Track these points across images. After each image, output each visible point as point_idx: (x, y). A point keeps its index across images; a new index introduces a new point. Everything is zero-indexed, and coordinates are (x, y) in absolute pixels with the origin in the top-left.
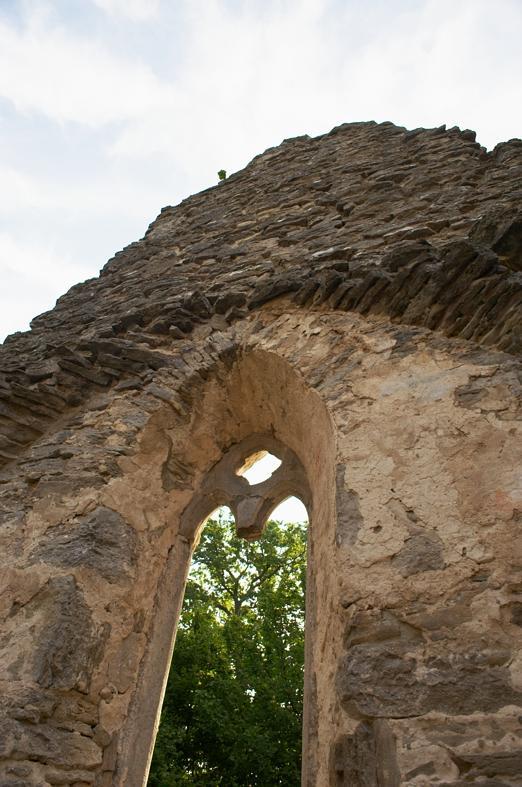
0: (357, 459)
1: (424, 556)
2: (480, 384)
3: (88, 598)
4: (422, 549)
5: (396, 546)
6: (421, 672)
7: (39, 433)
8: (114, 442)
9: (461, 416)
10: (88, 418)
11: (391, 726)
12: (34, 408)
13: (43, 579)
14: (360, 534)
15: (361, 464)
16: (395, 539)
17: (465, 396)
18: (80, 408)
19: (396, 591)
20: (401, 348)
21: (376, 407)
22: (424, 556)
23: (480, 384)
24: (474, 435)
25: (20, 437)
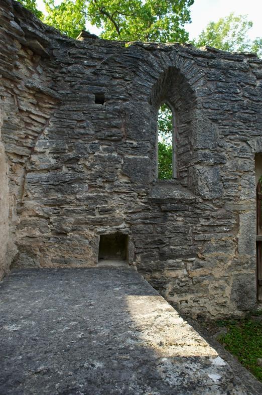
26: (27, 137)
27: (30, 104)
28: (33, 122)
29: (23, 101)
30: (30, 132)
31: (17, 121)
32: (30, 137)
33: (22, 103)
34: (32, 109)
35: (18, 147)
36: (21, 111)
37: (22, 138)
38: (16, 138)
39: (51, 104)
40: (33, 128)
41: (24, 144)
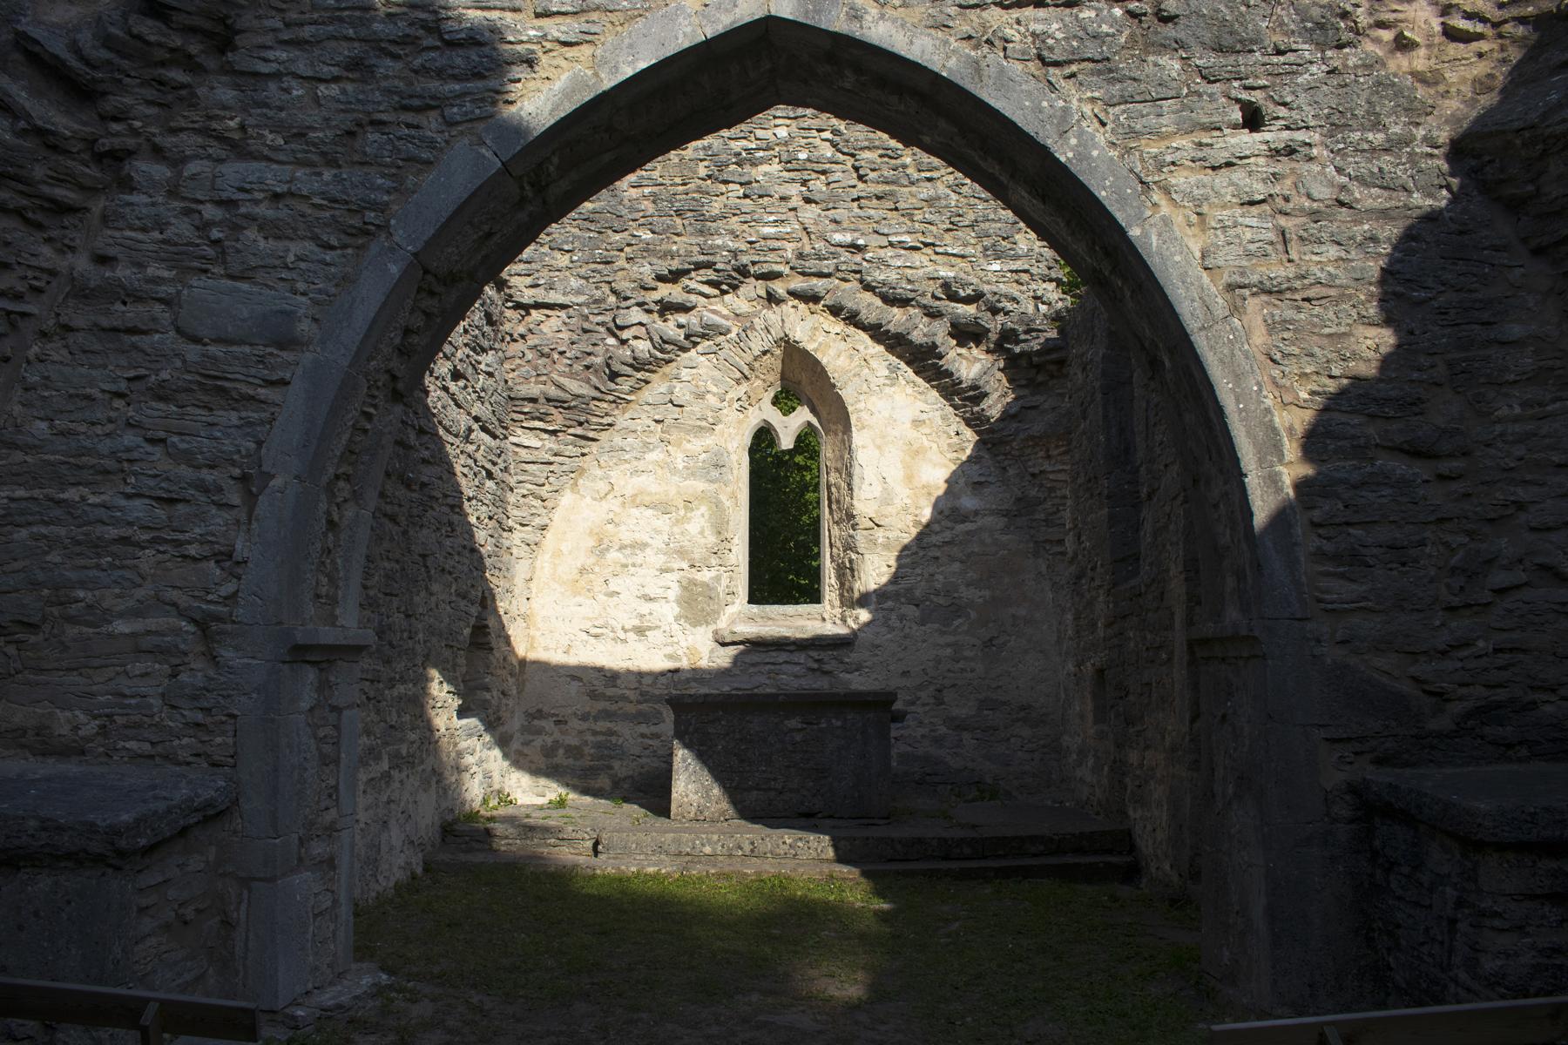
0: (863, 447)
1: (887, 500)
2: (924, 416)
3: (723, 498)
4: (885, 495)
5: (877, 494)
6: (880, 540)
7: (647, 382)
8: (712, 400)
9: (912, 434)
10: (685, 374)
11: (866, 556)
12: (646, 367)
13: (702, 489)
14: (863, 486)
15: (865, 450)
16: (877, 490)
17: (917, 423)
18: (674, 364)
19: (876, 512)
20: (893, 379)
21: (874, 417)
22: (887, 500)
23: (924, 416)
24: (915, 446)
25: (637, 386)
26: (1058, 511)
27: (1040, 461)
28: (1055, 484)
29: (1029, 460)
30: (1057, 501)
31: (1033, 492)
32: (1061, 508)
33: (1030, 463)
34: (1047, 466)
35: (1051, 530)
36: (1033, 475)
37: (1051, 514)
38: (1042, 516)
39: (1063, 446)
40: (1059, 493)
41: (1059, 522)
